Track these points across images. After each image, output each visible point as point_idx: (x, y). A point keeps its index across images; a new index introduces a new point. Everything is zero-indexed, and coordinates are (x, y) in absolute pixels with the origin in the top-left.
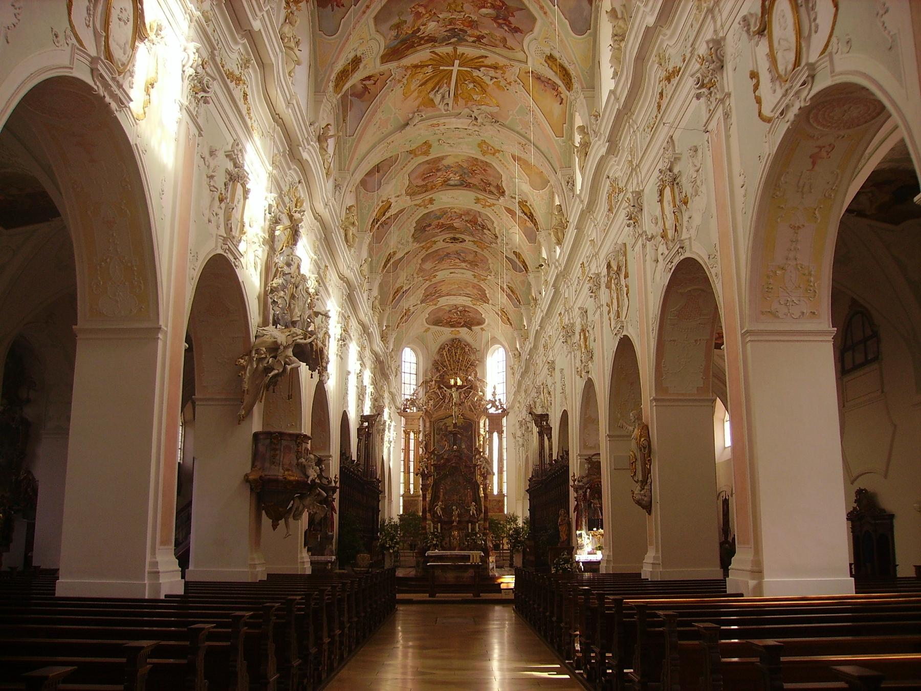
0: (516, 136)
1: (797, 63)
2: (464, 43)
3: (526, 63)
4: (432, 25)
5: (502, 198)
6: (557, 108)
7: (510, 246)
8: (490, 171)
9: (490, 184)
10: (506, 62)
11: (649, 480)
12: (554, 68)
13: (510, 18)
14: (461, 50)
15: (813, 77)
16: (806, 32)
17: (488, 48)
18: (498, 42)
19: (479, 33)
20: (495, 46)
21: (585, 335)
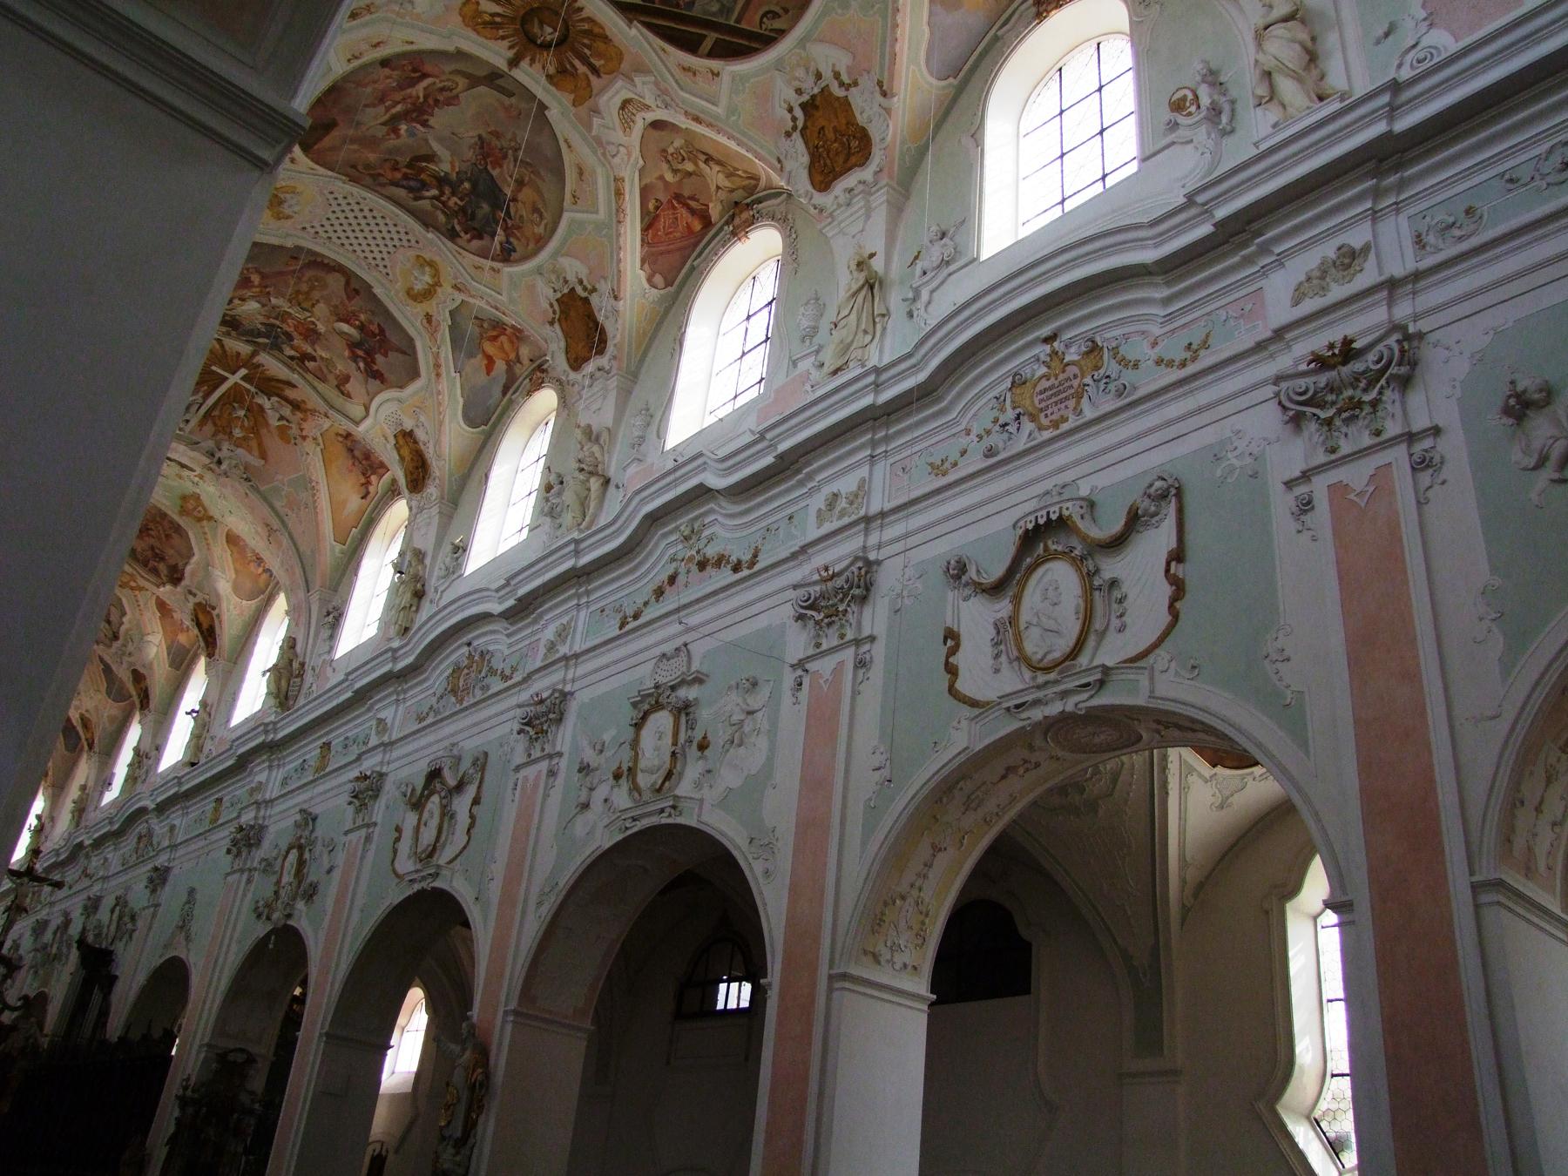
0: (266, 510)
1: (1075, 653)
2: (276, 353)
3: (357, 423)
4: (253, 306)
5: (168, 587)
6: (354, 502)
7: (131, 659)
8: (176, 540)
9: (162, 559)
10: (322, 406)
11: (471, 1140)
12: (406, 452)
13: (379, 358)
14: (264, 358)
15: (1102, 683)
16: (1098, 625)
17: (310, 377)
18: (331, 378)
19: (310, 350)
20: (323, 380)
21: (301, 855)
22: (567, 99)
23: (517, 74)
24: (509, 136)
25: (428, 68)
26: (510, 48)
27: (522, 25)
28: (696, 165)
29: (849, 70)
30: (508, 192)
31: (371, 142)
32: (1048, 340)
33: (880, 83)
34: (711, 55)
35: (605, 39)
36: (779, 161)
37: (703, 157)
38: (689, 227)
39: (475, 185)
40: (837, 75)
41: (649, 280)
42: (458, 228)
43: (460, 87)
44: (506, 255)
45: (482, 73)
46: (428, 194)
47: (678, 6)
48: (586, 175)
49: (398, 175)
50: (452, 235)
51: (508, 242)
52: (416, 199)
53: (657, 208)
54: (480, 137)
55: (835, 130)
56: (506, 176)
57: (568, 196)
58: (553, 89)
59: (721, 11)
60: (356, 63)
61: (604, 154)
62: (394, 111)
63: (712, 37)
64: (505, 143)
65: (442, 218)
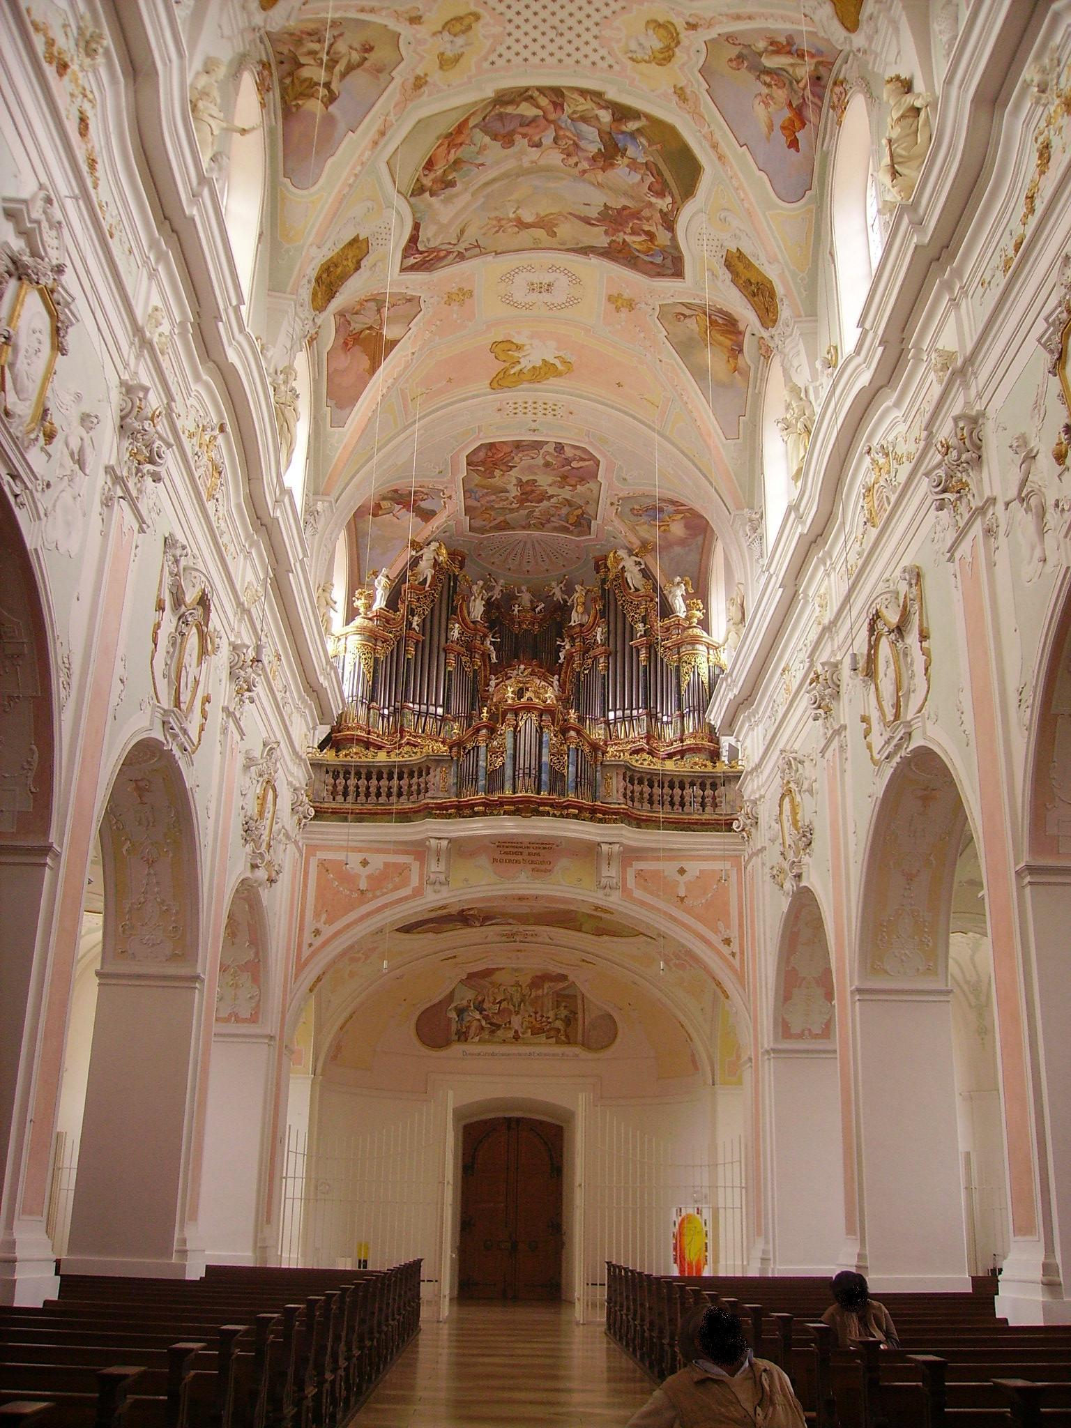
32: (222, 429)
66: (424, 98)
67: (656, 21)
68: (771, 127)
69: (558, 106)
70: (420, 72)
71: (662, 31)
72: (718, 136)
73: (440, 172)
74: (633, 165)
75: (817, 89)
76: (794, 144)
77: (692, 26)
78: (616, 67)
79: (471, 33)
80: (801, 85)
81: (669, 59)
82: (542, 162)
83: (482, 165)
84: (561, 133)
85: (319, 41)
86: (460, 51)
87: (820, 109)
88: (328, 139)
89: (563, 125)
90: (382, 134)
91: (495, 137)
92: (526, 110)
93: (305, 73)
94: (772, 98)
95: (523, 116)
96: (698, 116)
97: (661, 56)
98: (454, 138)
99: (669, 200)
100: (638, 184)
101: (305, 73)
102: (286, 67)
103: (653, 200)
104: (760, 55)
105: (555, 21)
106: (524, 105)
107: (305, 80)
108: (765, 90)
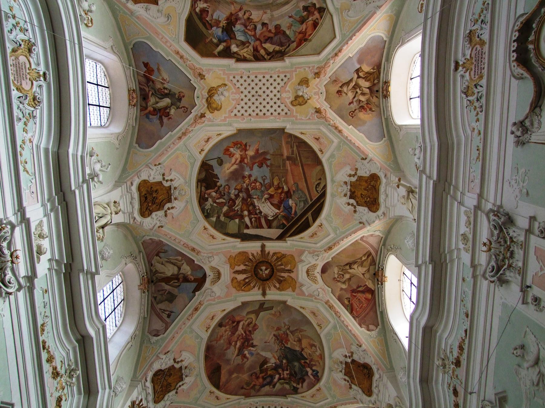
22: (289, 291)
23: (268, 297)
24: (283, 325)
25: (237, 318)
26: (259, 289)
27: (257, 277)
28: (349, 273)
29: (351, 169)
30: (297, 349)
31: (239, 368)
33: (363, 159)
34: (314, 220)
35: (284, 256)
36: (360, 223)
37: (348, 267)
38: (366, 299)
39: (286, 357)
40: (350, 176)
41: (368, 330)
42: (295, 385)
43: (254, 319)
44: (317, 378)
45: (257, 307)
46: (276, 380)
47: (293, 218)
48: (316, 312)
49: (261, 380)
50: (295, 391)
51: (313, 371)
52: (274, 386)
53: (349, 301)
54: (274, 335)
55: (365, 189)
56: (292, 344)
57: (317, 328)
58: (283, 292)
59: (304, 203)
60: (210, 331)
61: (316, 298)
62: (238, 346)
63: (309, 215)
64: (284, 330)
65: (287, 386)
66: (316, 66)
67: (218, 110)
68: (158, 69)
69: (256, 50)
70: (317, 80)
71: (214, 106)
72: (181, 61)
73: (310, 19)
74: (218, 22)
75: (143, 93)
76: (146, 65)
77: (203, 116)
78: (231, 78)
79: (295, 95)
80: (151, 93)
81: (210, 91)
82: (261, 12)
83: (290, 17)
84: (253, 33)
85: (360, 101)
86: (300, 87)
87: (139, 84)
88: (362, 55)
89: (253, 38)
90: (336, 55)
91: (284, 32)
92: (270, 47)
93: (367, 84)
94: (162, 83)
95: (271, 43)
96: (193, 69)
97: (213, 91)
98: (304, 39)
99: (198, 10)
100: (214, 11)
101: (367, 84)
102: (376, 89)
103: (205, 5)
104: (172, 104)
105: (260, 100)
106: (271, 50)
107: (368, 81)
108: (166, 86)
